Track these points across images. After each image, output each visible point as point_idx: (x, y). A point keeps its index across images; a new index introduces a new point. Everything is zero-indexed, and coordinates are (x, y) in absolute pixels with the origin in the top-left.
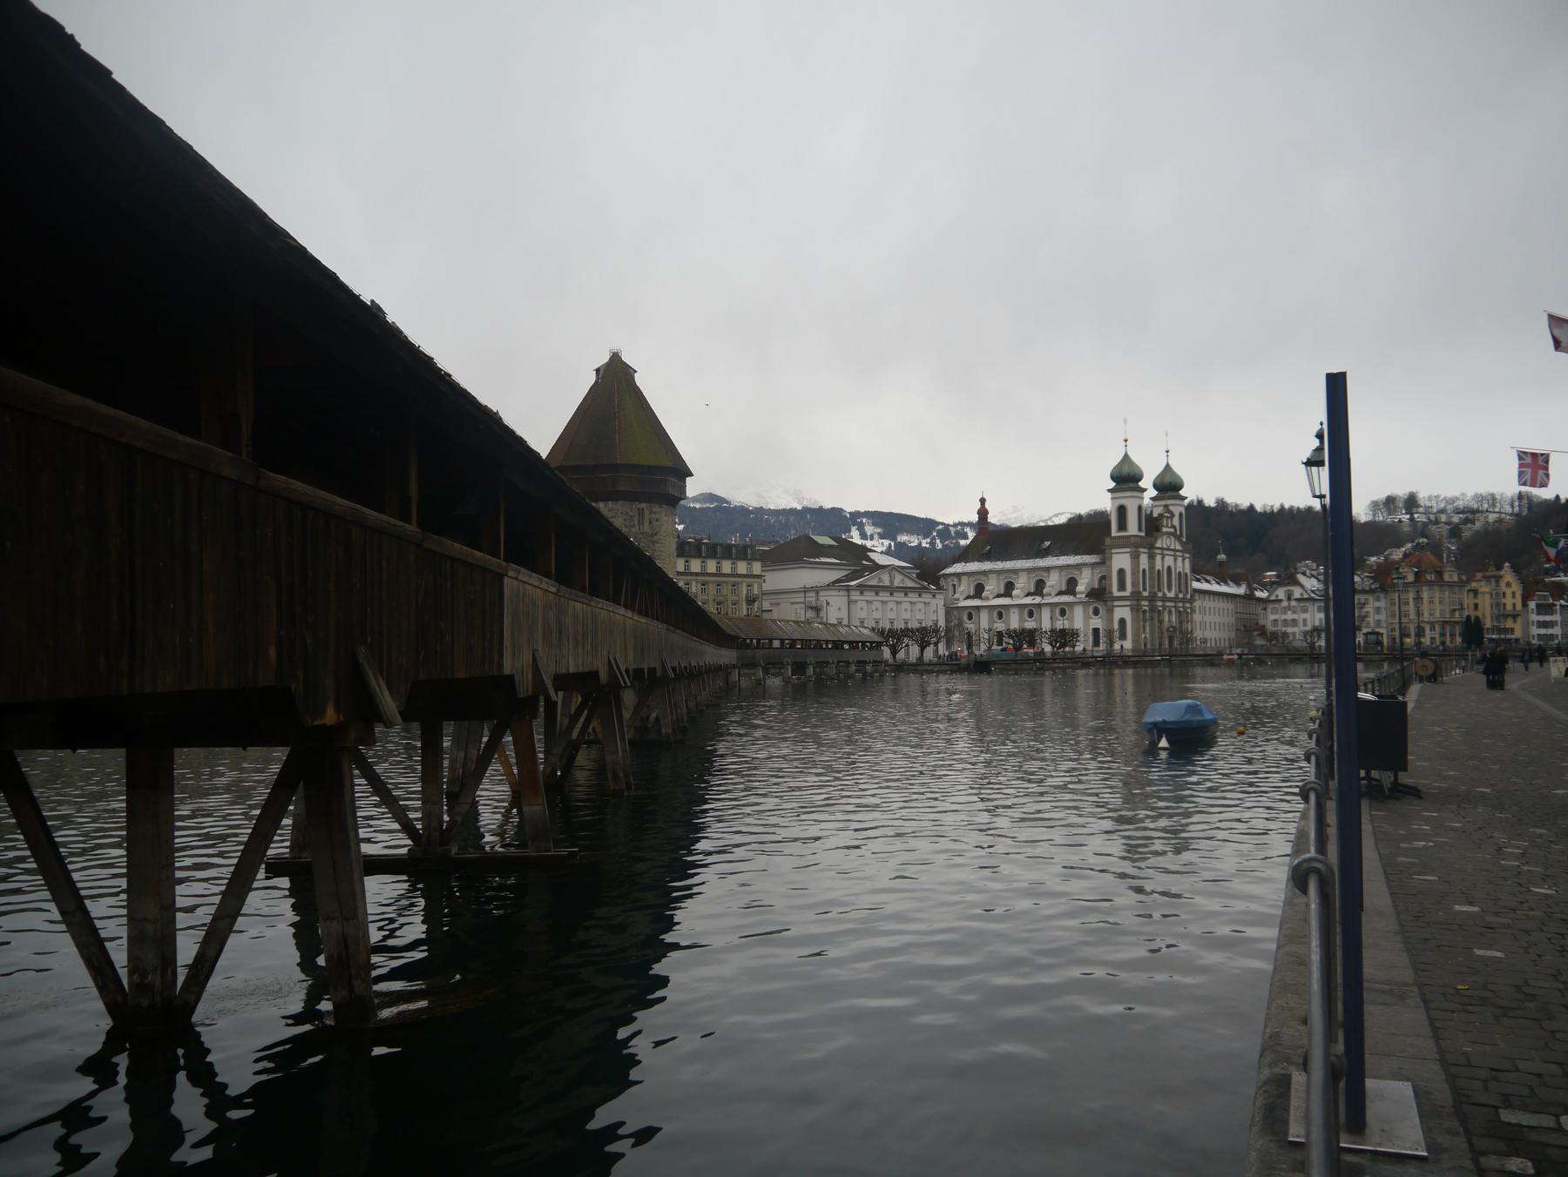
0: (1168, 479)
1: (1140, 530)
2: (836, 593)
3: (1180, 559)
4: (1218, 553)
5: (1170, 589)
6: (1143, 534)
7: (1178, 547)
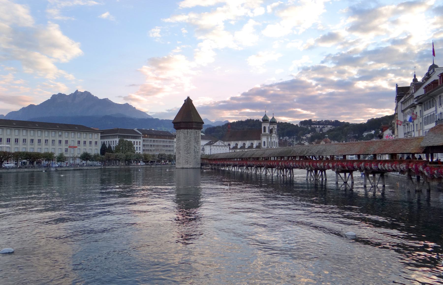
0: (273, 120)
1: (269, 132)
2: (208, 147)
3: (276, 139)
4: (281, 137)
5: (274, 146)
6: (269, 133)
7: (276, 136)
